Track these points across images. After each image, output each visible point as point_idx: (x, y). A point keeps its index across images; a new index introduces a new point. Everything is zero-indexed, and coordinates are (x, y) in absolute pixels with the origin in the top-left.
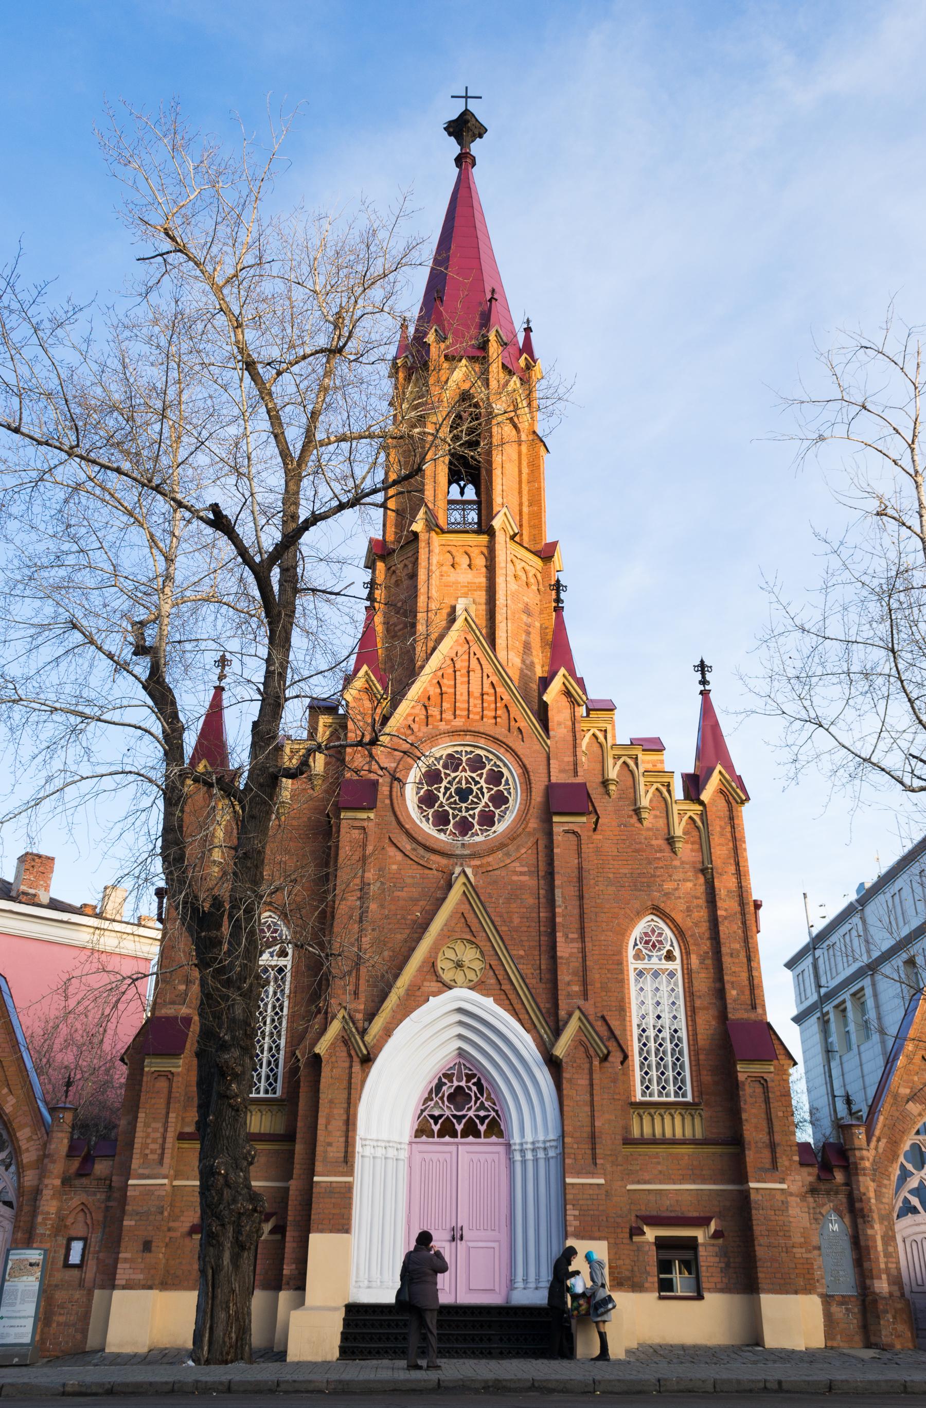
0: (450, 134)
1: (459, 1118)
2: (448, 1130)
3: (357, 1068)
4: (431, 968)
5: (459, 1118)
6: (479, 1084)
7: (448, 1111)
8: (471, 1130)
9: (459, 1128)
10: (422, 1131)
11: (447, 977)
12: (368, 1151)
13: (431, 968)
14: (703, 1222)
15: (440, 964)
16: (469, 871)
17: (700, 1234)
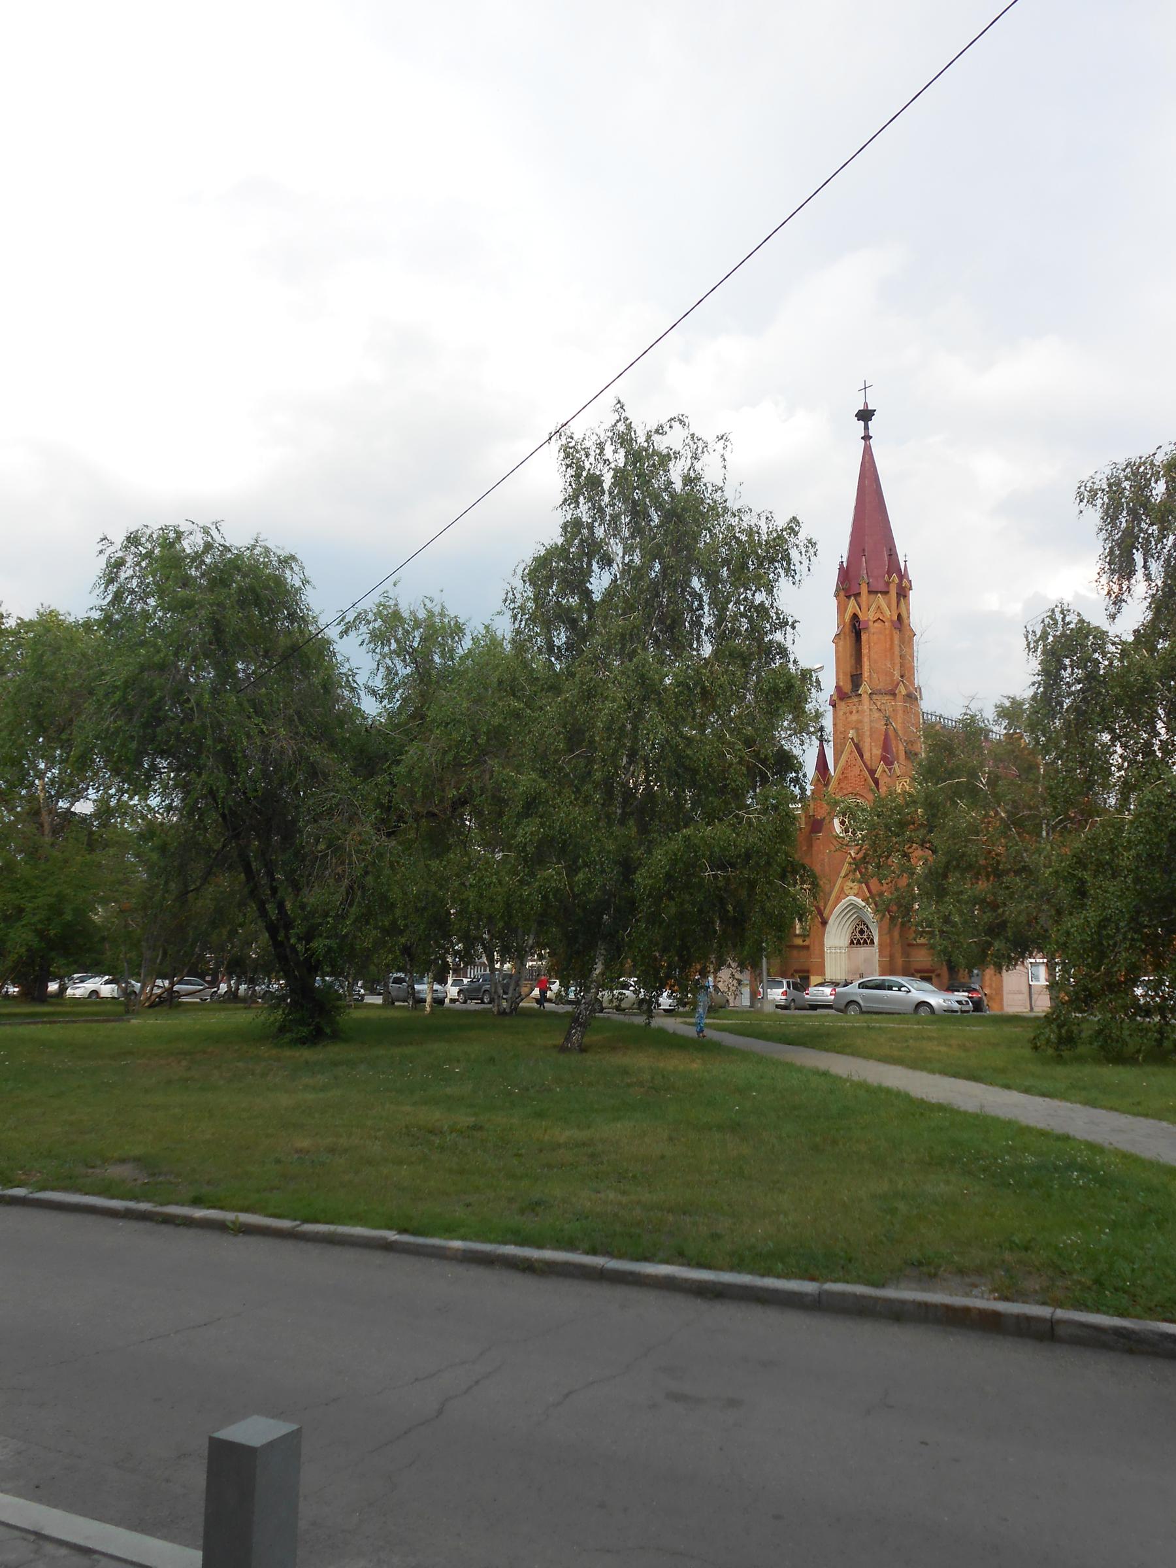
0: (858, 420)
1: (862, 939)
2: (858, 942)
3: (820, 926)
4: (842, 890)
5: (862, 939)
6: (867, 927)
7: (859, 936)
8: (865, 942)
9: (862, 942)
10: (852, 942)
11: (847, 893)
12: (829, 951)
13: (842, 890)
14: (932, 971)
15: (845, 888)
16: (852, 852)
17: (933, 975)
